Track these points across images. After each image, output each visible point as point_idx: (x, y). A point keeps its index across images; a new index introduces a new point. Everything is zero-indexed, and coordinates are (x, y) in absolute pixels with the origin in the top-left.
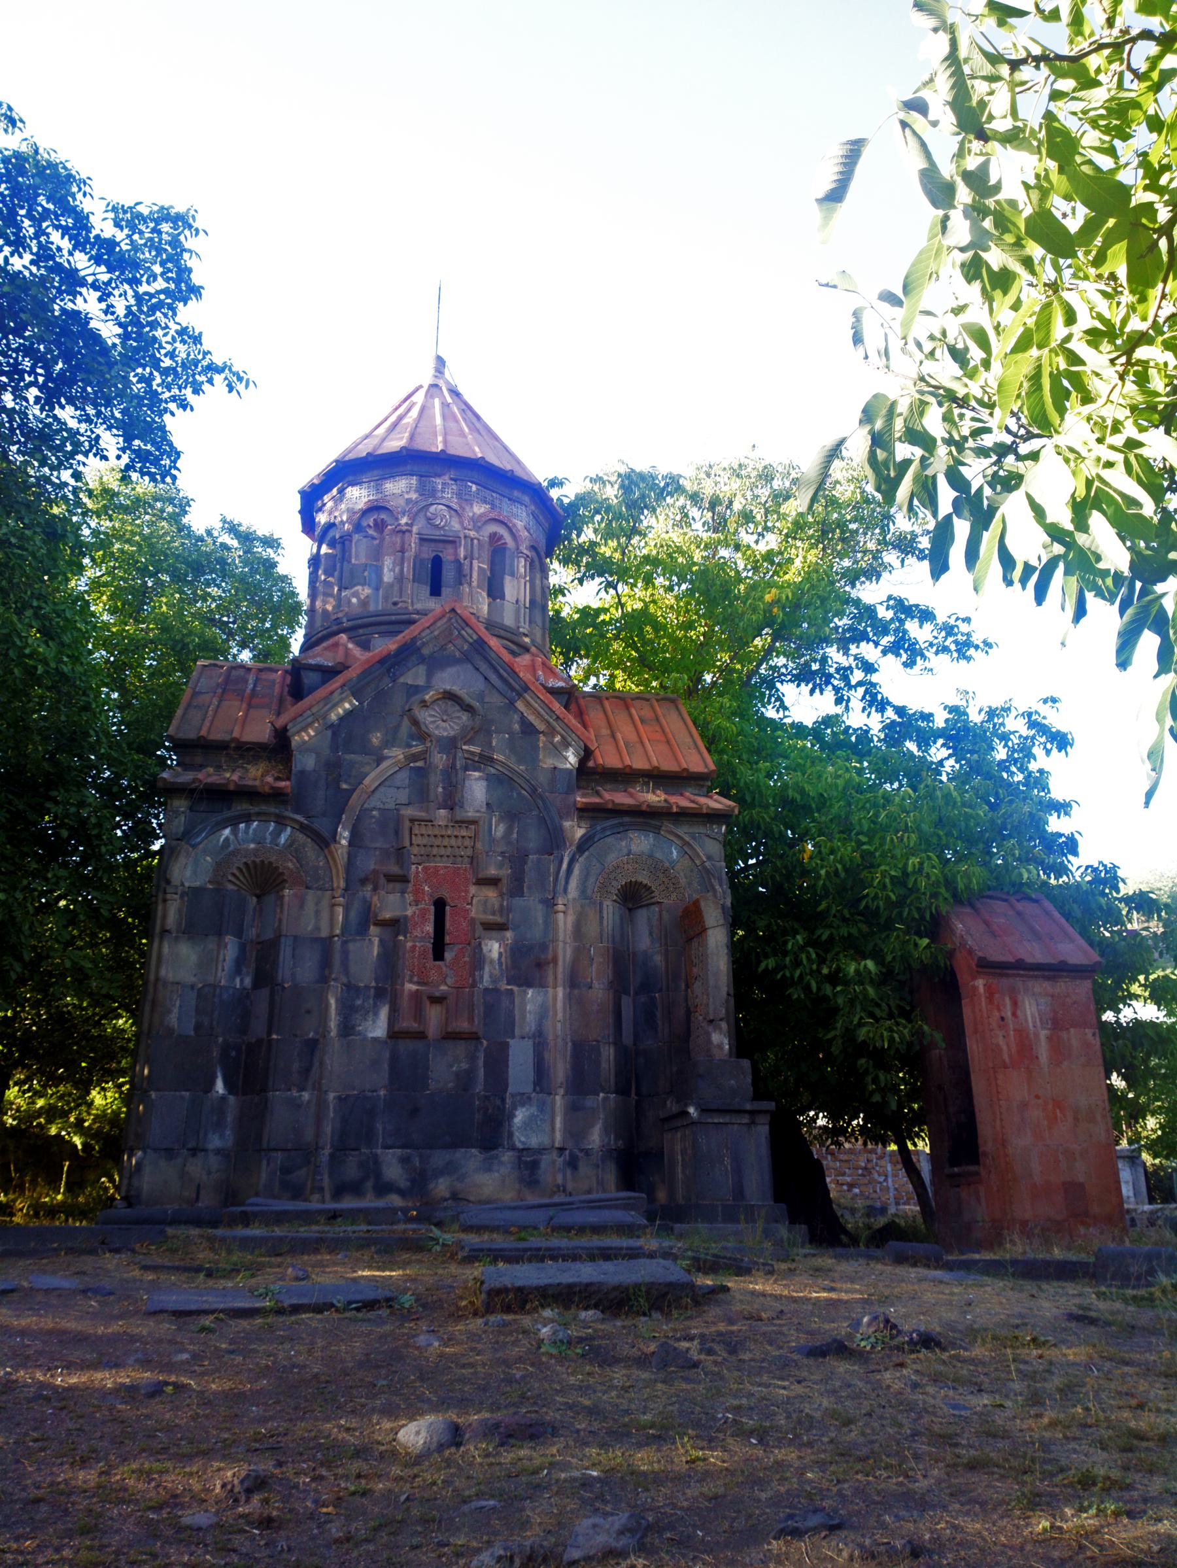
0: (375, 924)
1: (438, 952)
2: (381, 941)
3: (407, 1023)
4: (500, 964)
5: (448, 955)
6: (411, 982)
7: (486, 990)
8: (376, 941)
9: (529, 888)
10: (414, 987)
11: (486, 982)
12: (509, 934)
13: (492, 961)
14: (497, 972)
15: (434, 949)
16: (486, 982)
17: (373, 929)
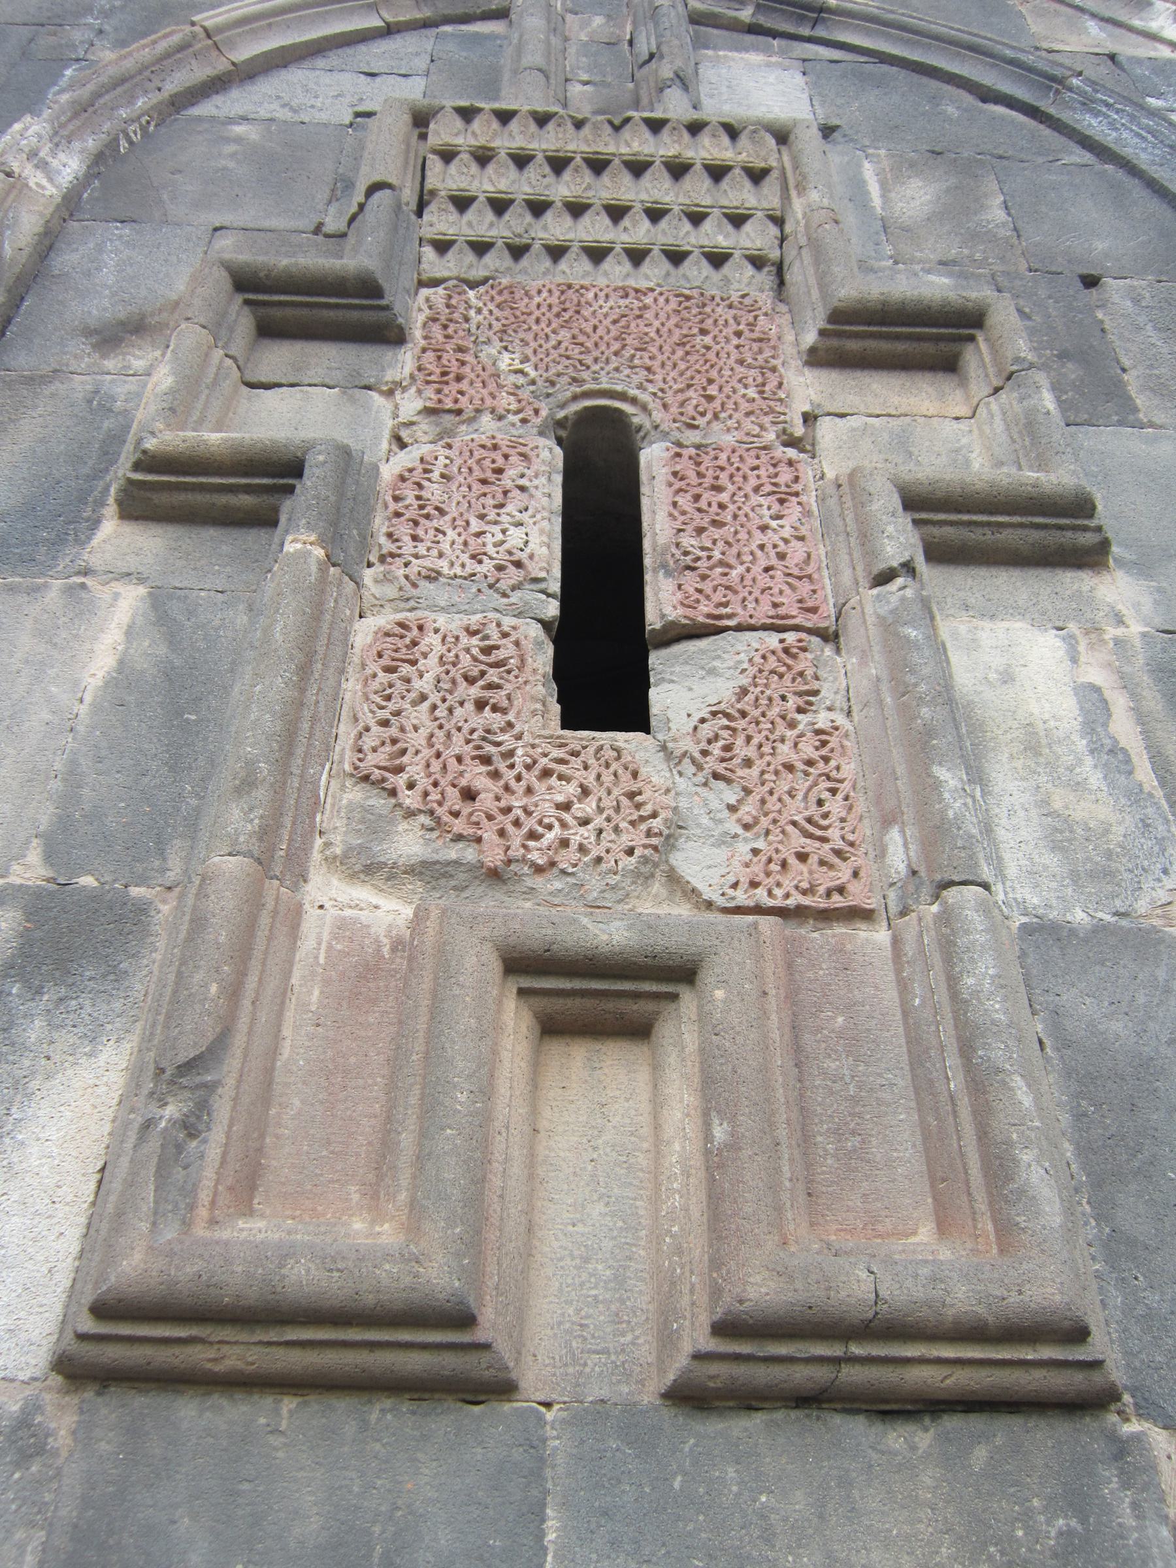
0: (138, 506)
1: (603, 664)
2: (163, 608)
3: (327, 1229)
4: (1114, 757)
5: (681, 690)
6: (368, 868)
7: (1042, 933)
8: (126, 604)
9: (1159, 389)
10: (387, 911)
11: (1027, 875)
12: (1116, 590)
13: (1034, 744)
14: (1097, 807)
15: (566, 634)
16: (1027, 875)
17: (113, 538)
